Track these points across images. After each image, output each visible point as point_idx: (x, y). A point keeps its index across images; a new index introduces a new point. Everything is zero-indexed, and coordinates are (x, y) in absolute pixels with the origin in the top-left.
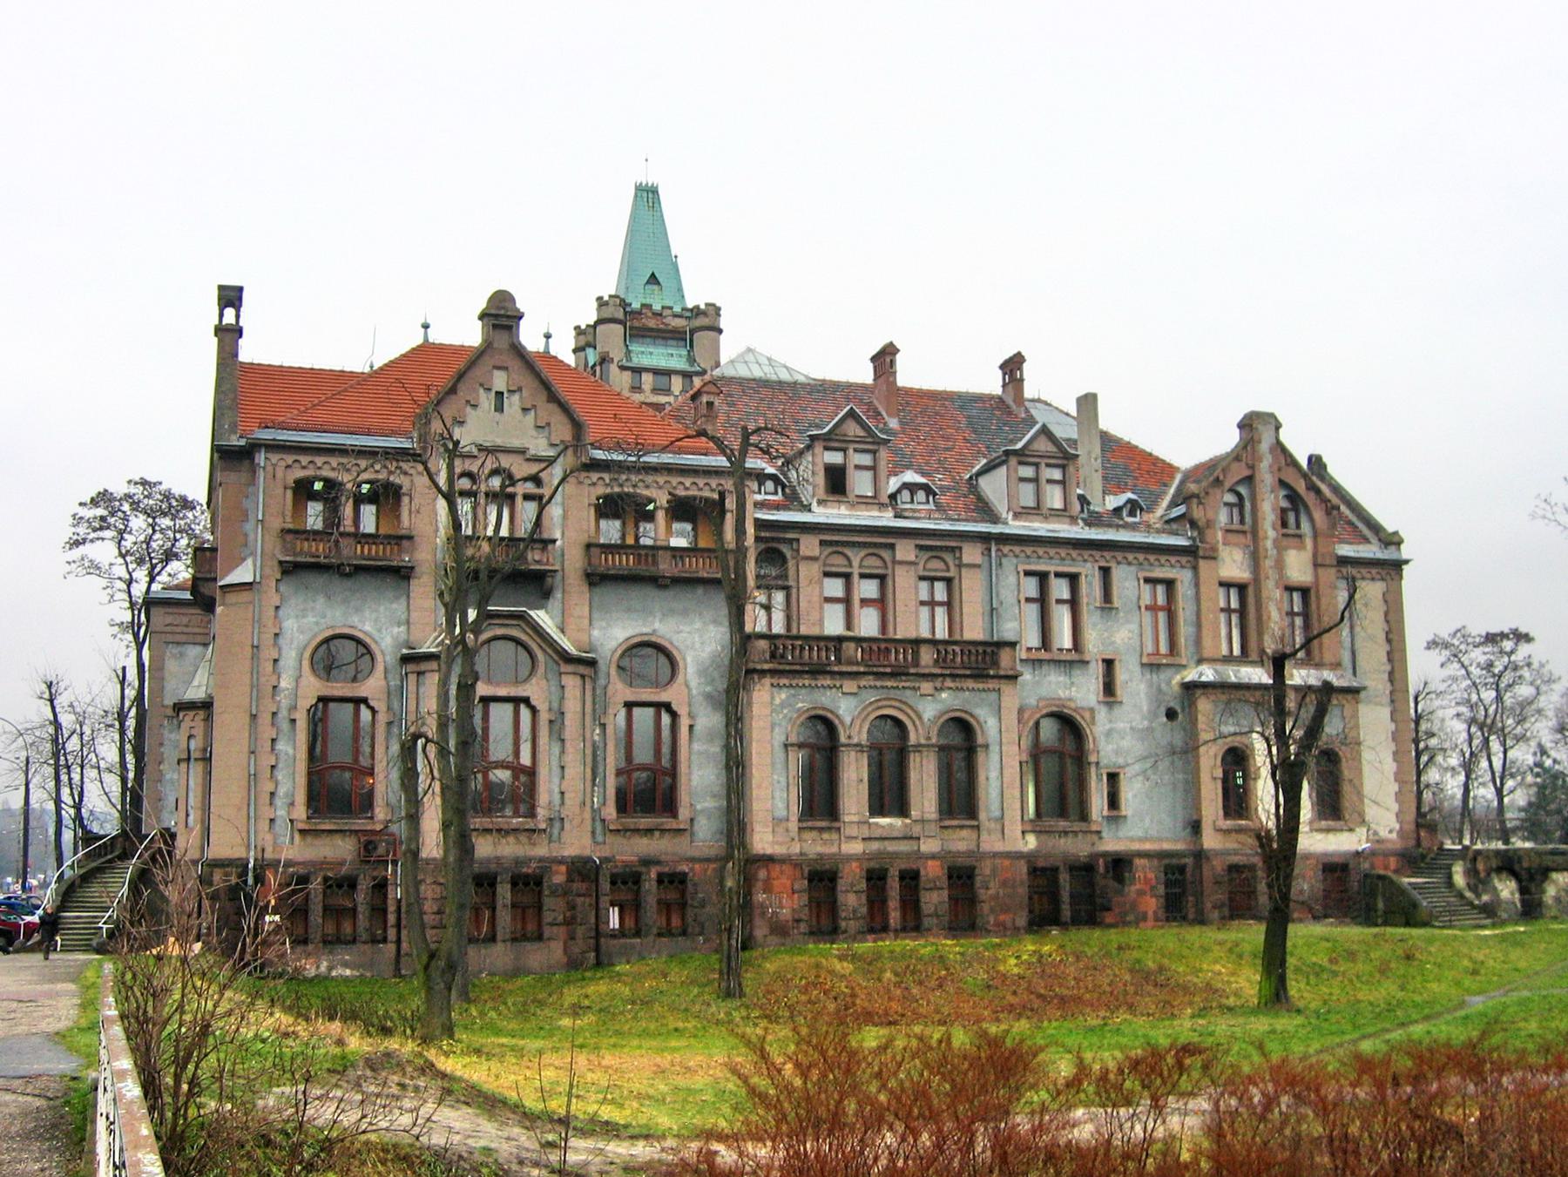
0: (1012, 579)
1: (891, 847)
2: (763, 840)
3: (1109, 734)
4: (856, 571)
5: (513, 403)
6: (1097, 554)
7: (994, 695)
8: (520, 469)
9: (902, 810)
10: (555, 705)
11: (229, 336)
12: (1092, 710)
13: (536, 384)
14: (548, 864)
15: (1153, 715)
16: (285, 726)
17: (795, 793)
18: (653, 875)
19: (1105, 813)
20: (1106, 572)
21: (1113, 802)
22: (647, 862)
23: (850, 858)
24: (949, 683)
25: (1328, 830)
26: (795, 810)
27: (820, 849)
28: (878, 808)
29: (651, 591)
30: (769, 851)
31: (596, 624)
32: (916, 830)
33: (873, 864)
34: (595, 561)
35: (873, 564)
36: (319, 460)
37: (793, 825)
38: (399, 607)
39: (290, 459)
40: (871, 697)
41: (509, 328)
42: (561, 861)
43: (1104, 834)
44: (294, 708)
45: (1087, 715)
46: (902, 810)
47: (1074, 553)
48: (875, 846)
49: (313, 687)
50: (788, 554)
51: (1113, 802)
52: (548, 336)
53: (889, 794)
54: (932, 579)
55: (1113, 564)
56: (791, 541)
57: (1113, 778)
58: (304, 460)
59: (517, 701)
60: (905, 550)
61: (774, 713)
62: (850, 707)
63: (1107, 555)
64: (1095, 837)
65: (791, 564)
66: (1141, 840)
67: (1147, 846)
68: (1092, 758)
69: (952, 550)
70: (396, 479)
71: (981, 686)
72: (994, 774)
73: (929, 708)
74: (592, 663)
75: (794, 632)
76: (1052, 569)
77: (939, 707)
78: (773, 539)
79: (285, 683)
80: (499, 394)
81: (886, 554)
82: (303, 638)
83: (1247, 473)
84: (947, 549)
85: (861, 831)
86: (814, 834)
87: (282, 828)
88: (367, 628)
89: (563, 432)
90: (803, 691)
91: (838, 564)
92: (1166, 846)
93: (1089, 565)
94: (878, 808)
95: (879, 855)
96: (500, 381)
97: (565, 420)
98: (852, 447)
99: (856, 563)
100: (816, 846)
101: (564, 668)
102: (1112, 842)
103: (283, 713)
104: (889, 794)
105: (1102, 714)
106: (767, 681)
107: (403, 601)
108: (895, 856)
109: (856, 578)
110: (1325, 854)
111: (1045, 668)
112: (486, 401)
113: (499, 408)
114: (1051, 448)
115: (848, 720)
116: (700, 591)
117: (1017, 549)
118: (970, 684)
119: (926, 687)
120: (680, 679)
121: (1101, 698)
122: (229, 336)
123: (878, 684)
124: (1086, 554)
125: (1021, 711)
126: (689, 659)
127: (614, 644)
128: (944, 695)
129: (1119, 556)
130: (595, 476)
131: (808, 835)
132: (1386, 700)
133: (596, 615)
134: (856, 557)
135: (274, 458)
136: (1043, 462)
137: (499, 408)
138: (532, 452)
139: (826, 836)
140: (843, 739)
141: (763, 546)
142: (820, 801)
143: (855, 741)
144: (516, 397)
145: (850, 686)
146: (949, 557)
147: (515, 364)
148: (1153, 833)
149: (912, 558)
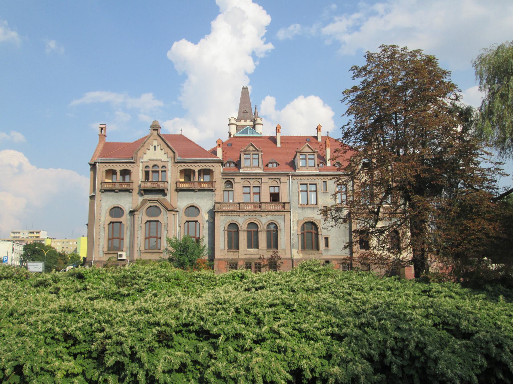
0: (297, 186)
1: (253, 256)
2: (218, 255)
4: (251, 186)
5: (158, 148)
6: (322, 178)
7: (283, 216)
8: (160, 164)
9: (257, 247)
10: (166, 222)
11: (102, 136)
13: (164, 143)
16: (102, 228)
17: (226, 243)
21: (327, 245)
23: (241, 259)
26: (226, 247)
27: (233, 257)
28: (249, 246)
29: (192, 193)
32: (260, 252)
33: (247, 260)
34: (178, 186)
35: (257, 184)
36: (111, 165)
38: (130, 200)
39: (104, 165)
40: (248, 217)
41: (157, 130)
43: (323, 254)
44: (104, 225)
45: (318, 222)
46: (257, 247)
47: (315, 178)
48: (249, 256)
49: (110, 219)
50: (233, 182)
51: (327, 245)
53: (253, 243)
54: (274, 187)
55: (327, 180)
56: (233, 179)
57: (326, 239)
58: (107, 165)
59: (196, 222)
60: (265, 179)
61: (222, 222)
62: (242, 221)
63: (325, 178)
64: (321, 255)
65: (234, 184)
66: (334, 256)
68: (319, 233)
69: (279, 178)
70: (129, 168)
72: (283, 237)
73: (263, 221)
74: (177, 211)
75: (252, 201)
76: (308, 182)
78: (228, 178)
79: (102, 219)
80: (155, 146)
81: (260, 180)
82: (107, 208)
84: (277, 178)
85: (245, 252)
86: (232, 254)
87: (101, 253)
88: (122, 205)
89: (172, 154)
91: (247, 184)
94: (249, 246)
95: (249, 258)
96: (155, 143)
97: (171, 151)
98: (251, 153)
99: (251, 183)
100: (231, 256)
101: (168, 212)
102: (326, 255)
103: (102, 226)
104: (253, 243)
106: (219, 214)
107: (131, 198)
108: (253, 259)
109: (252, 187)
111: (306, 209)
112: (152, 148)
113: (155, 149)
114: (310, 150)
115: (241, 224)
116: (206, 192)
117: (298, 178)
118: (276, 213)
119: (263, 214)
120: (200, 214)
122: (102, 136)
124: (319, 178)
125: (298, 221)
126: (203, 210)
127: (184, 206)
128: (269, 217)
130: (179, 165)
131: (229, 254)
134: (252, 181)
135: (101, 165)
136: (307, 154)
137: (155, 149)
138: (163, 160)
139: (235, 254)
140: (240, 229)
141: (226, 180)
142: (233, 244)
143: (243, 229)
144: (159, 146)
145: (242, 215)
146: (278, 181)
147: (159, 139)
148: (338, 254)
149: (267, 181)
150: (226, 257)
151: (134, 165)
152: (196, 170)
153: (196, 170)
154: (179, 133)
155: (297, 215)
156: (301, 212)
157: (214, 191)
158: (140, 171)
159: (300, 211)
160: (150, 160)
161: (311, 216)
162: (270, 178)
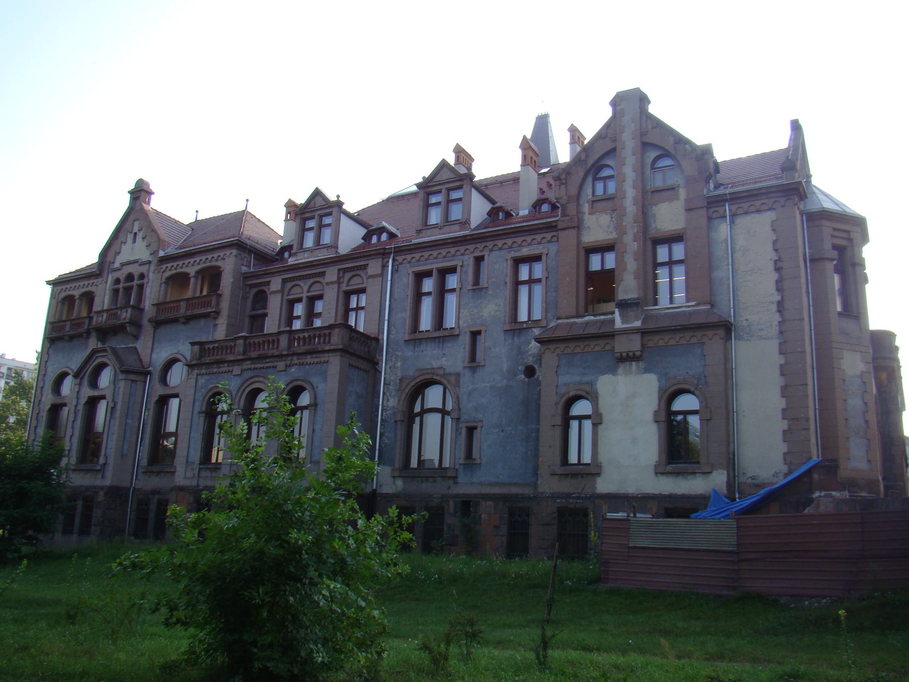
3: (470, 394)
5: (140, 236)
6: (471, 247)
12: (458, 375)
14: (96, 489)
15: (513, 374)
18: (155, 500)
19: (462, 461)
20: (479, 260)
22: (154, 492)
24: (295, 360)
25: (677, 474)
30: (182, 484)
31: (155, 351)
37: (196, 467)
42: (102, 488)
43: (460, 480)
52: (247, 200)
55: (486, 253)
64: (451, 482)
66: (491, 484)
67: (497, 490)
70: (90, 289)
71: (316, 360)
77: (289, 378)
83: (610, 146)
90: (214, 376)
92: (514, 490)
93: (466, 257)
105: (466, 378)
110: (671, 497)
112: (130, 237)
113: (134, 241)
116: (202, 322)
118: (309, 359)
121: (466, 364)
123: (253, 366)
128: (293, 370)
129: (490, 244)
131: (204, 474)
132: (775, 331)
133: (156, 345)
137: (134, 241)
141: (254, 291)
145: (237, 370)
150: (195, 483)
151: (100, 280)
152: (192, 271)
153: (192, 271)
154: (242, 208)
155: (399, 364)
156: (410, 354)
157: (215, 318)
158: (107, 292)
159: (409, 352)
160: (123, 265)
161: (435, 364)
162: (345, 270)
